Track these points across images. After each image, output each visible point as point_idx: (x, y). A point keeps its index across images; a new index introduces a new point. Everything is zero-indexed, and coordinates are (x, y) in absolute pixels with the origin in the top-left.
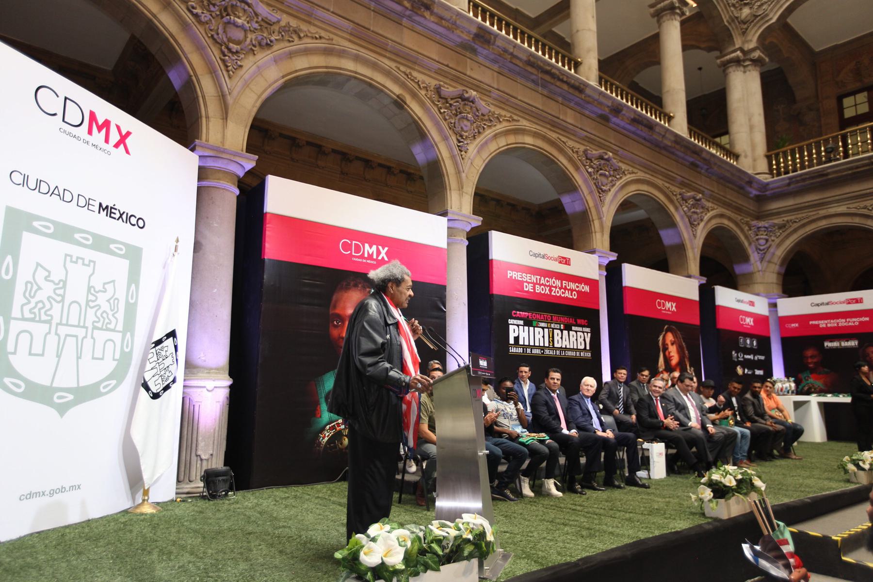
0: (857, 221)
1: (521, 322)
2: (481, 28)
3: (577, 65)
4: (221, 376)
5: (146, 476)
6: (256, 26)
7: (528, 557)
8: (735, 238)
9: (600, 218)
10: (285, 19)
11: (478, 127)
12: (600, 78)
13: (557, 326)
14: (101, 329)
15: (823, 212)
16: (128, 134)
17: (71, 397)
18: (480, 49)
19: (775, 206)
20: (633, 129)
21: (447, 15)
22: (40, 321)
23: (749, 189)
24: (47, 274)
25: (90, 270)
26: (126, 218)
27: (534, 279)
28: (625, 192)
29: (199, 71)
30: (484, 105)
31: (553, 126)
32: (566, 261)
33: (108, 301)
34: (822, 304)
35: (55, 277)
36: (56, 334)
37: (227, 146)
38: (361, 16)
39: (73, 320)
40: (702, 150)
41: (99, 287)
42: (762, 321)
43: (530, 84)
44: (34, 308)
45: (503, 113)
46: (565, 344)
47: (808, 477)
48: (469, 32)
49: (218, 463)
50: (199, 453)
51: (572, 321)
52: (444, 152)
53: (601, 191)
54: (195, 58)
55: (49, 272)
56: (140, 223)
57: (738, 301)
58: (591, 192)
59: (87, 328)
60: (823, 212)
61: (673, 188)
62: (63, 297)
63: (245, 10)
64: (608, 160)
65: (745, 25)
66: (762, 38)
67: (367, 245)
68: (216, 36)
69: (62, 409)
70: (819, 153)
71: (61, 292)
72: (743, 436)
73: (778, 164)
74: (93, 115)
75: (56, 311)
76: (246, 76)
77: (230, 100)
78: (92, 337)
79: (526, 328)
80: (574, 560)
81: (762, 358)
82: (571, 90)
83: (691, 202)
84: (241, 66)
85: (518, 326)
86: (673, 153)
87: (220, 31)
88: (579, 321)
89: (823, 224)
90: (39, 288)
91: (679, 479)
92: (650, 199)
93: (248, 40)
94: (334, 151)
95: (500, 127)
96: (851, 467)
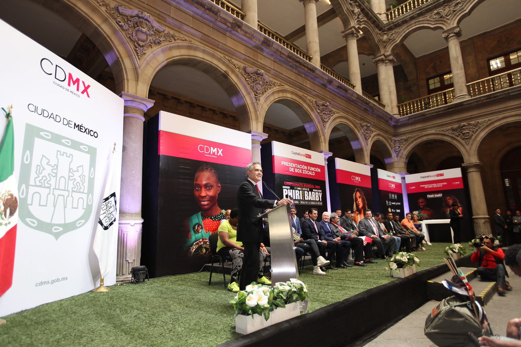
0: (439, 137)
1: (289, 187)
2: (265, 38)
3: (310, 59)
4: (137, 218)
5: (102, 272)
6: (153, 33)
7: (317, 301)
8: (385, 145)
9: (324, 135)
10: (167, 30)
11: (264, 88)
12: (321, 66)
13: (306, 189)
14: (76, 192)
15: (424, 133)
16: (89, 86)
17: (61, 229)
18: (265, 49)
19: (403, 130)
20: (338, 91)
21: (249, 31)
22: (45, 187)
23: (390, 122)
24: (48, 161)
25: (70, 159)
26: (88, 131)
27: (294, 165)
28: (335, 122)
29: (123, 56)
30: (267, 77)
31: (300, 89)
32: (309, 157)
33: (80, 176)
34: (426, 177)
35: (52, 163)
37: (139, 95)
38: (206, 30)
39: (62, 187)
40: (370, 102)
41: (75, 169)
42: (398, 186)
43: (289, 68)
44: (42, 179)
45: (277, 81)
46: (310, 198)
47: (429, 258)
48: (260, 40)
49: (137, 264)
50: (127, 259)
51: (313, 187)
52: (248, 101)
53: (324, 122)
54: (120, 48)
55: (49, 160)
56: (95, 135)
57: (388, 176)
58: (319, 122)
59: (69, 191)
60: (424, 133)
61: (357, 121)
62: (56, 174)
63: (147, 24)
64: (327, 106)
65: (385, 43)
66: (393, 50)
67: (212, 148)
68: (131, 37)
69: (57, 236)
70: (421, 104)
71: (54, 171)
72: (398, 240)
73: (403, 110)
74: (70, 75)
75: (53, 181)
76: (148, 59)
77: (139, 71)
78: (72, 196)
79: (291, 190)
80: (341, 300)
81: (399, 204)
82: (309, 71)
83: (365, 128)
84: (145, 54)
85: (287, 189)
86: (356, 104)
87: (134, 35)
88: (316, 187)
89: (425, 138)
90: (44, 169)
91: (436, 244)
92: (346, 126)
93: (149, 40)
94: (186, 102)
95: (275, 89)
96: (450, 252)
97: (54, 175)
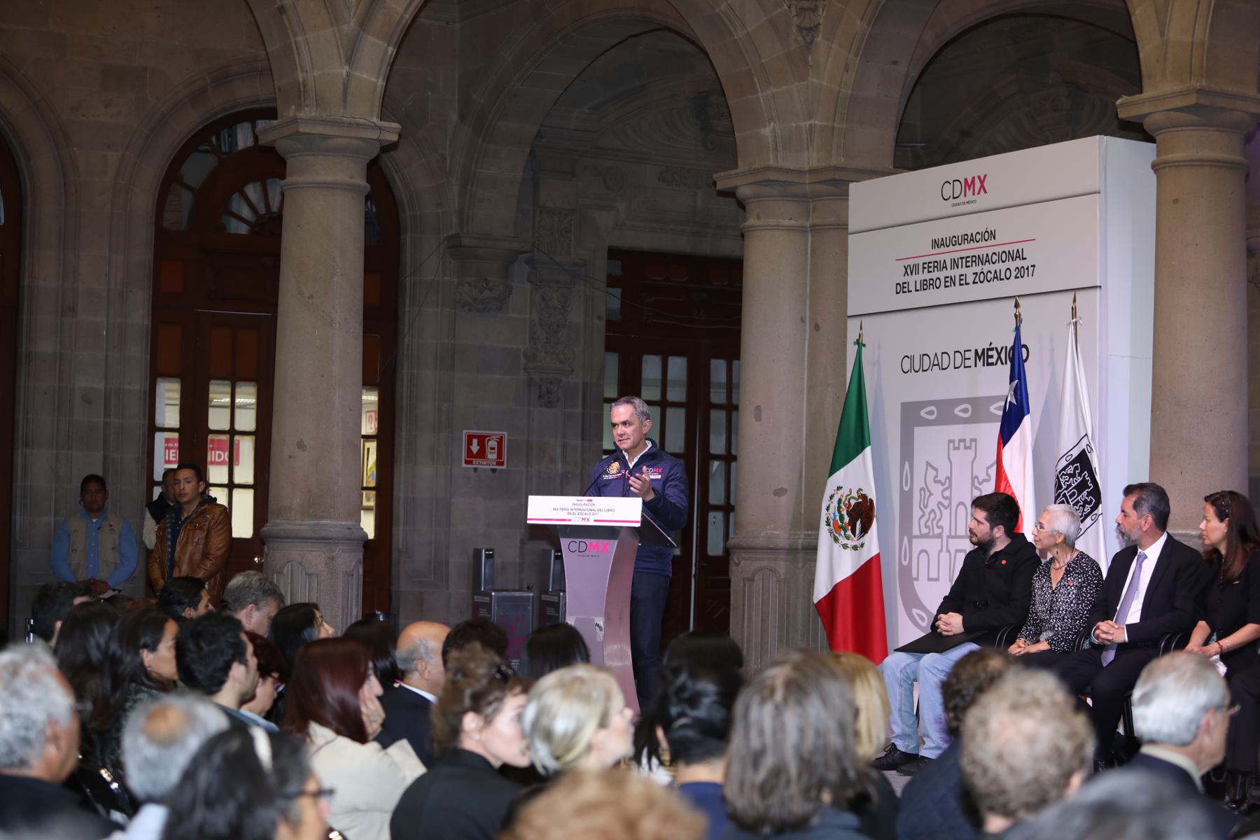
36: (948, 551)
62: (949, 498)
71: (947, 494)
75: (945, 523)
90: (931, 494)
97: (946, 503)
